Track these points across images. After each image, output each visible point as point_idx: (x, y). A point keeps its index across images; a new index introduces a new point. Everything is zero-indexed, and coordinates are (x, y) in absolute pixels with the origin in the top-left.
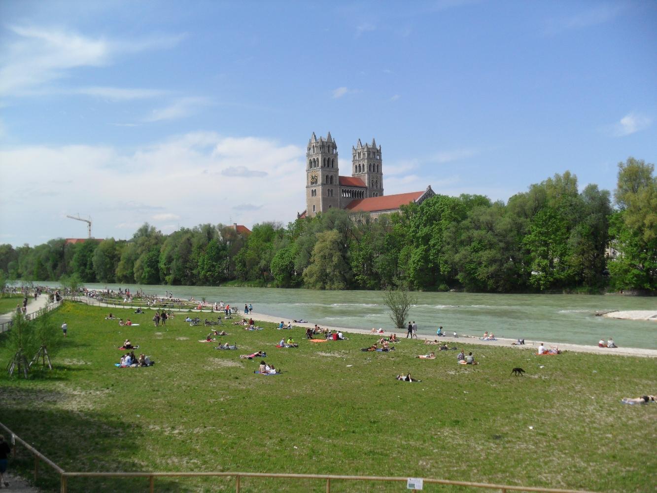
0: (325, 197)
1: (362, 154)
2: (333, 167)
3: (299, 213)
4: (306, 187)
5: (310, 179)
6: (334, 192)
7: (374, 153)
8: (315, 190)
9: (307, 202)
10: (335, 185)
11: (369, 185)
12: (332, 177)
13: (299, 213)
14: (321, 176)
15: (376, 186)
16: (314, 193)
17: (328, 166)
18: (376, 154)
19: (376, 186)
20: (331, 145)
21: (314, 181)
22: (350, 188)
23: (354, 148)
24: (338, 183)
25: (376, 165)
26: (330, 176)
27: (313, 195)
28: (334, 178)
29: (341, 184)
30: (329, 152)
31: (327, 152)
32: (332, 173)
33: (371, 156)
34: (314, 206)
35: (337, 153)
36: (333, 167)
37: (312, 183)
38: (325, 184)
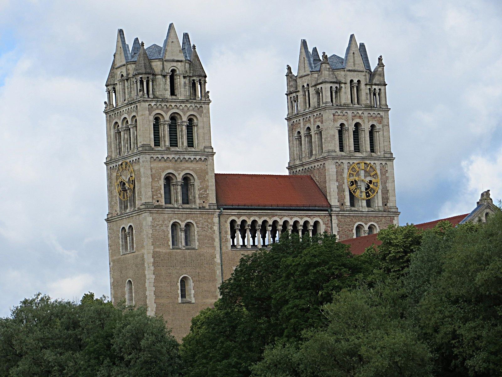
0: (163, 250)
1: (312, 90)
2: (191, 143)
4: (107, 220)
6: (196, 230)
7: (355, 86)
9: (112, 270)
12: (186, 179)
17: (174, 142)
18: (364, 89)
20: (180, 68)
22: (260, 216)
24: (212, 199)
25: (366, 127)
26: (180, 178)
28: (197, 183)
29: (222, 205)
30: (173, 93)
31: (169, 92)
32: (187, 165)
33: (345, 96)
35: (206, 95)
36: (191, 143)
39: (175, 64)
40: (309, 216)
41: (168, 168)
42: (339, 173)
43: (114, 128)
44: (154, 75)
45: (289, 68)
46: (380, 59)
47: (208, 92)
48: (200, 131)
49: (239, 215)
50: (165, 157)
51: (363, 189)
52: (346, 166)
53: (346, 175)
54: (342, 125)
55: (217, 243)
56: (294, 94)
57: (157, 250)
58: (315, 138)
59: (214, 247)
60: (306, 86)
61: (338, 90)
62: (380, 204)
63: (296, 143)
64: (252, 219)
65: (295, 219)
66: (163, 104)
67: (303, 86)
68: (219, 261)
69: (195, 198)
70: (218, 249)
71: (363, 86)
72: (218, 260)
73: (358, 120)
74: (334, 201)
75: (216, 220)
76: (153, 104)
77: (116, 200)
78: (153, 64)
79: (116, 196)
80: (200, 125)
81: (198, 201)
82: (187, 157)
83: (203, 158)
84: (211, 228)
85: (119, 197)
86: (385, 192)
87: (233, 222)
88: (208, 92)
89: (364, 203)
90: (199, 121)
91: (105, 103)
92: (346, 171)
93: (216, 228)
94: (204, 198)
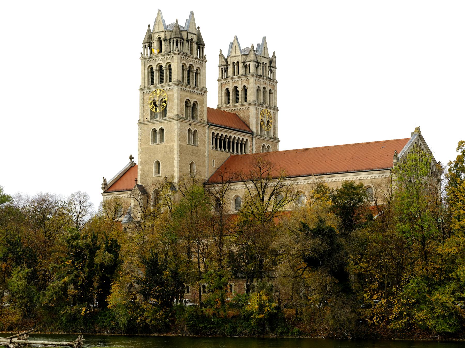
1: (241, 65)
3: (105, 180)
5: (149, 107)
6: (198, 135)
7: (264, 66)
8: (162, 130)
10: (200, 122)
11: (257, 128)
13: (105, 180)
14: (176, 101)
15: (268, 133)
16: (158, 134)
19: (268, 133)
21: (158, 109)
23: (221, 55)
27: (154, 141)
28: (199, 108)
31: (189, 51)
32: (195, 96)
34: (158, 163)
35: (205, 57)
37: (153, 115)
38: (182, 118)
39: (193, 35)
40: (244, 136)
41: (187, 96)
42: (257, 113)
43: (148, 69)
44: (183, 40)
45: (221, 51)
46: (274, 53)
47: (206, 55)
48: (202, 77)
49: (216, 130)
50: (187, 89)
51: (266, 125)
52: (260, 110)
53: (259, 116)
54: (258, 87)
55: (206, 145)
56: (226, 67)
57: (181, 144)
58: (241, 93)
59: (205, 146)
60: (236, 62)
61: (258, 67)
62: (272, 135)
63: (224, 94)
64: (221, 133)
65: (239, 136)
66: (187, 58)
67: (234, 63)
68: (207, 155)
69: (197, 116)
70: (207, 148)
71: (267, 67)
72: (206, 154)
73: (265, 86)
74: (254, 130)
75: (207, 131)
76: (182, 57)
77: (147, 112)
78: (183, 33)
79: (147, 110)
80: (201, 74)
81: (199, 118)
82: (196, 91)
83: (203, 93)
84: (205, 135)
85: (151, 111)
86: (274, 128)
87: (213, 133)
88: (206, 55)
89: (266, 133)
90: (201, 72)
91: (141, 53)
92: (259, 113)
93: (206, 135)
94: (202, 117)
